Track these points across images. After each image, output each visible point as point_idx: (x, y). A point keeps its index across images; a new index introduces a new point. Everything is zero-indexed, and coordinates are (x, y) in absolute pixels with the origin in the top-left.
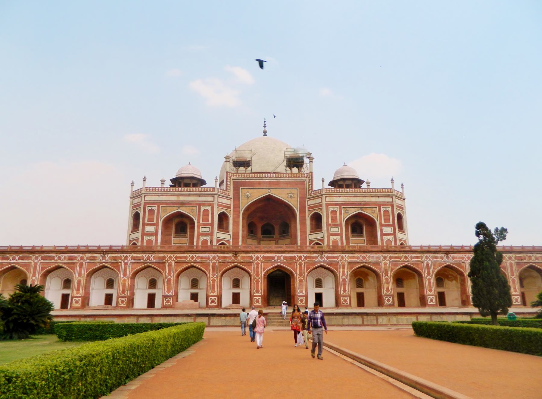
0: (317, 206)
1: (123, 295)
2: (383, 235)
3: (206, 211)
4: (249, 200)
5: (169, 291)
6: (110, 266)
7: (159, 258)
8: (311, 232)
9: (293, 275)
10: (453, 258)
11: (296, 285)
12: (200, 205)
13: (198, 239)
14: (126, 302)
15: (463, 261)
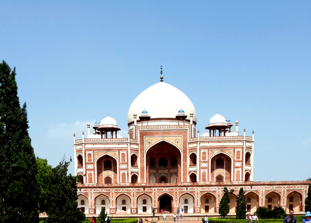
0: (194, 149)
1: (91, 208)
2: (235, 167)
3: (123, 154)
4: (150, 145)
5: (113, 206)
6: (83, 194)
7: (107, 190)
8: (190, 166)
9: (172, 198)
10: (254, 188)
11: (174, 203)
12: (119, 150)
13: (119, 172)
14: (93, 211)
15: (259, 189)
